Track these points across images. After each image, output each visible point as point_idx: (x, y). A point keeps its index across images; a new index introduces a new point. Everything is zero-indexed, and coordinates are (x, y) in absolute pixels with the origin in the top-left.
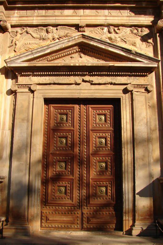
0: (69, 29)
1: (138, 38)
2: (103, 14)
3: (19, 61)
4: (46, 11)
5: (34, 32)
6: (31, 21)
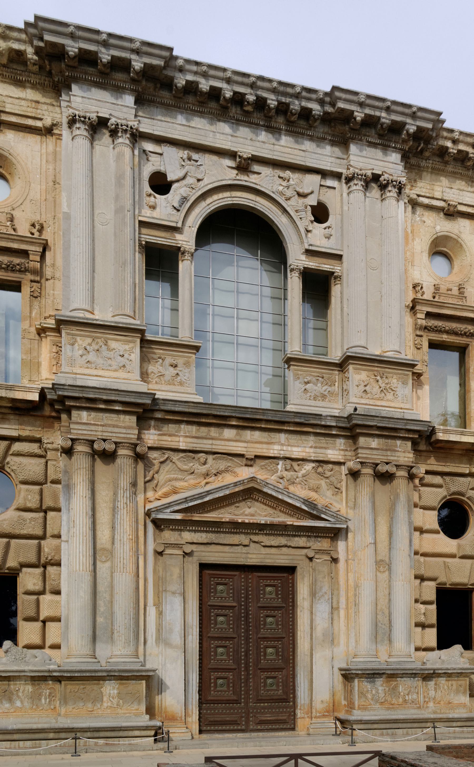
0: (231, 459)
1: (322, 479)
2: (278, 440)
3: (168, 510)
4: (198, 428)
5: (181, 461)
6: (177, 444)
